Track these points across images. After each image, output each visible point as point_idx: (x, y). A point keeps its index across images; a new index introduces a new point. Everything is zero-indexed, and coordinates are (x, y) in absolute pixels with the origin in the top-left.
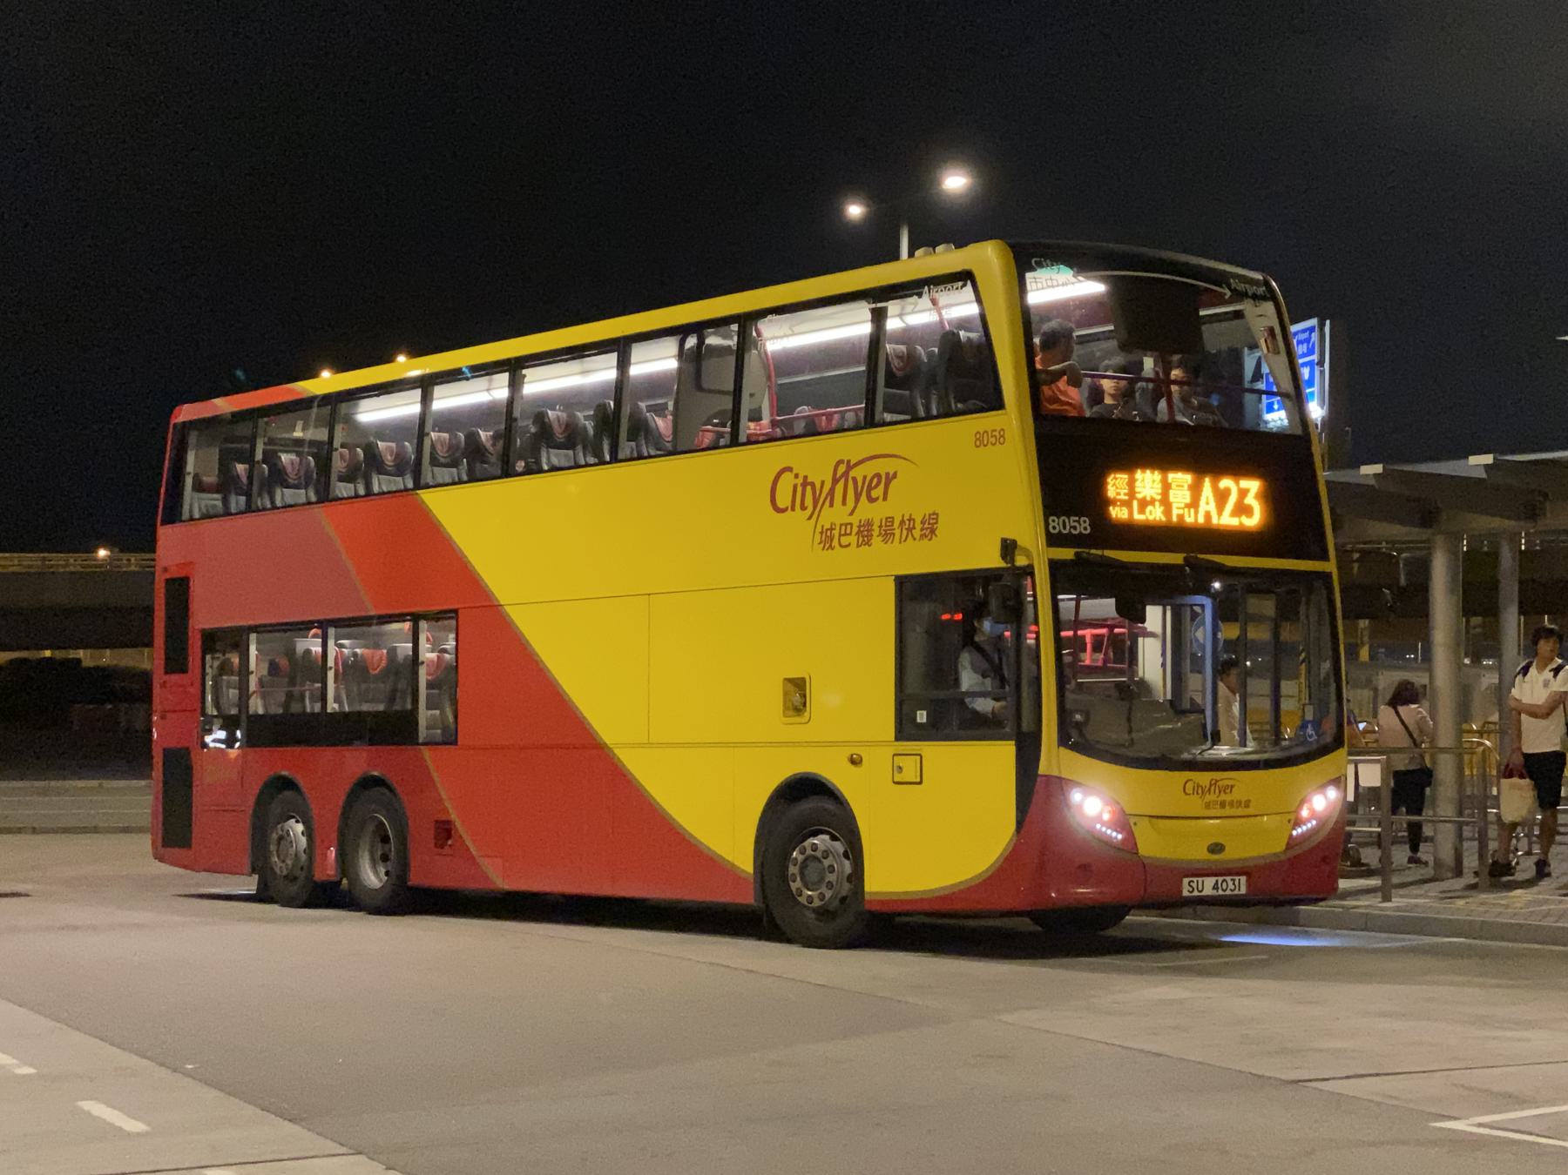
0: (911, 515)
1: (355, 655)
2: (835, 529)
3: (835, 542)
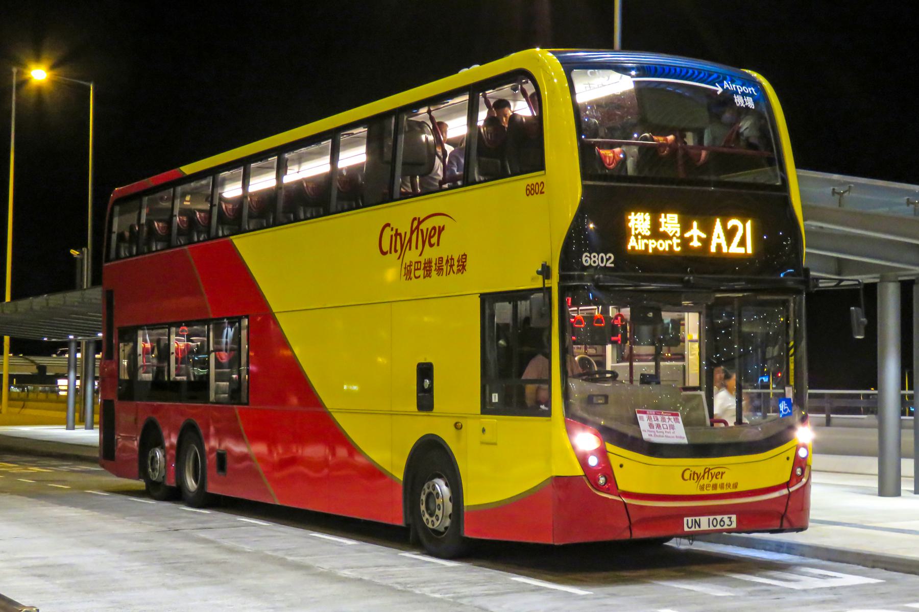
0: (452, 256)
1: (197, 345)
2: (412, 265)
3: (412, 275)
